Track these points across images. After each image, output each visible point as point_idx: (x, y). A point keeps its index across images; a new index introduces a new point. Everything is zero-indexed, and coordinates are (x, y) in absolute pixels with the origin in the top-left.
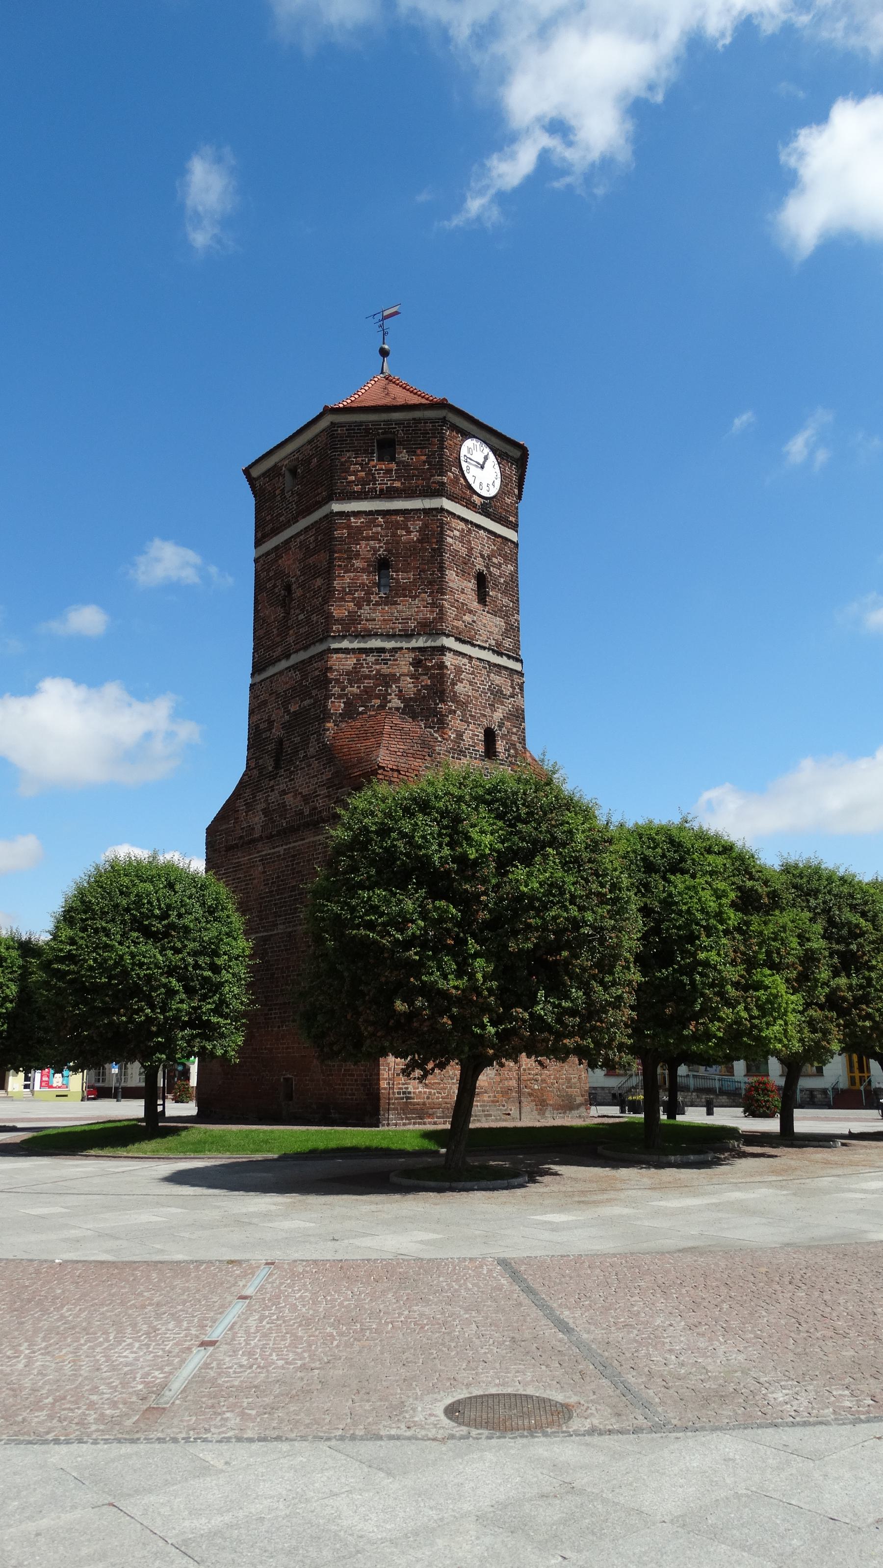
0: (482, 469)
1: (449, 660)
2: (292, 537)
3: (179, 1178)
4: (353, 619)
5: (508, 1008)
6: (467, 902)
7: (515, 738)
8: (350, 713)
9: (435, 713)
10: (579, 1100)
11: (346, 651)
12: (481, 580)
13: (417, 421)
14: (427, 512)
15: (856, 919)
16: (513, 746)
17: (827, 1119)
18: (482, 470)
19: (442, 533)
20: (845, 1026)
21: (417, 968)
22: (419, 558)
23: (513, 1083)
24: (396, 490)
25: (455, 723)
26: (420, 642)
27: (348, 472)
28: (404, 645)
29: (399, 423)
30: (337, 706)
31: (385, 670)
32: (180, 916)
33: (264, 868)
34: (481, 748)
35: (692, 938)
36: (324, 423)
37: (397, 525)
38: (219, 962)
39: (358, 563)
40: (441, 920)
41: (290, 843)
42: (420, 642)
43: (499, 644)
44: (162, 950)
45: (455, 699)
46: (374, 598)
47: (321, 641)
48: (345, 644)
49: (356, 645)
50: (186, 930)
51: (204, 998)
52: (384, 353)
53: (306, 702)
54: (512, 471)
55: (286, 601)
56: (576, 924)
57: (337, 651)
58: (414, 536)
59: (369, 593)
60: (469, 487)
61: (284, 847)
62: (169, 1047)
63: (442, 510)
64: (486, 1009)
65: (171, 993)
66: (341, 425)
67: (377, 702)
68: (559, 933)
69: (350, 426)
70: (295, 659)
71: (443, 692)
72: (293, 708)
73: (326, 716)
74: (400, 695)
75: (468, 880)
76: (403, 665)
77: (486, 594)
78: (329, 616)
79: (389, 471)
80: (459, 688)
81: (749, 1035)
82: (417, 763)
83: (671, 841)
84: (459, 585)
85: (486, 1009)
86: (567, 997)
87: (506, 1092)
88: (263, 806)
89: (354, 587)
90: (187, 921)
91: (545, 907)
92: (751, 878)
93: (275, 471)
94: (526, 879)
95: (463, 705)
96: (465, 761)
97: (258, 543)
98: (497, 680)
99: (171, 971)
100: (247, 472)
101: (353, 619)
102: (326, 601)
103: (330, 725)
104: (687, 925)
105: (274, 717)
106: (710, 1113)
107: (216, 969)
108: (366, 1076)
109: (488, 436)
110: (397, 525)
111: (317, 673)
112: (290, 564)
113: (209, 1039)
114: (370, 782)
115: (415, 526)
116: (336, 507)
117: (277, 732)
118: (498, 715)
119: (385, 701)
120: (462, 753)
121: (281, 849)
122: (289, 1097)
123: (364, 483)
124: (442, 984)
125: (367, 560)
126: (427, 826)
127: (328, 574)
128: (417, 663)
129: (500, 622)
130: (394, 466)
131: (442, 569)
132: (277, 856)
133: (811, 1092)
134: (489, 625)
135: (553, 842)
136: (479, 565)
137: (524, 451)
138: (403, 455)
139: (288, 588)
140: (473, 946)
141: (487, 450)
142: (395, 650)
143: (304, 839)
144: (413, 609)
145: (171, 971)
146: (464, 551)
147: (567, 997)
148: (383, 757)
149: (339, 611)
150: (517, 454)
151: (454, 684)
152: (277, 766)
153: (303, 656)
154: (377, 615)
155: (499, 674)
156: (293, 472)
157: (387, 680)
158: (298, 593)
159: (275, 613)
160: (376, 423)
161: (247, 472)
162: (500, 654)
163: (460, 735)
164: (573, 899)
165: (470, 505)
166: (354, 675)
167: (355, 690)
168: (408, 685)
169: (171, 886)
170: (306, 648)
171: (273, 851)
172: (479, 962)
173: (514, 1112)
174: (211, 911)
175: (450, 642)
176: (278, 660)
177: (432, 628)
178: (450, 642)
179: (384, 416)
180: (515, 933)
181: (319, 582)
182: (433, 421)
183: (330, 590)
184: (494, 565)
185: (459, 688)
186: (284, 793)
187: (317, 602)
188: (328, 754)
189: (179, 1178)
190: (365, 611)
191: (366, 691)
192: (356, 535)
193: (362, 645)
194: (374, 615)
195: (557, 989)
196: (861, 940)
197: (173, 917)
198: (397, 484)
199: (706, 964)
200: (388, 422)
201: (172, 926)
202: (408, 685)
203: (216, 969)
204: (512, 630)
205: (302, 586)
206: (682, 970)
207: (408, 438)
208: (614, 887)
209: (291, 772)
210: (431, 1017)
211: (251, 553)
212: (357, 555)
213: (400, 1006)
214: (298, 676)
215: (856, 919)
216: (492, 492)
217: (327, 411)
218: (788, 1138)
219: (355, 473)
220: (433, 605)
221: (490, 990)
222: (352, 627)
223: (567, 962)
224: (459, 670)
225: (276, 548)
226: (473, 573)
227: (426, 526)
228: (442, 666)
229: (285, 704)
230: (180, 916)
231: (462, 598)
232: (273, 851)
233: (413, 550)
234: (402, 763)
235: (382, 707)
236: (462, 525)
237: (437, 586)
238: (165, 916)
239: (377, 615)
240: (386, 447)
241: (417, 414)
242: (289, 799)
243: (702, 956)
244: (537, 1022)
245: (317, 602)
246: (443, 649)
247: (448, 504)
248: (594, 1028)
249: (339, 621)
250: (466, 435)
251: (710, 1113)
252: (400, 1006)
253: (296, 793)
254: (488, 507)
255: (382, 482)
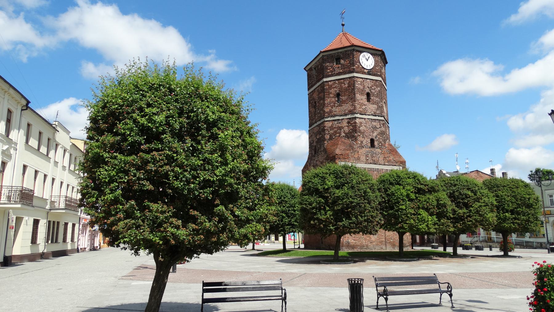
0: (367, 61)
1: (357, 121)
3: (278, 261)
4: (331, 111)
5: (337, 222)
6: (326, 198)
7: (381, 140)
8: (331, 138)
9: (354, 136)
10: (407, 244)
11: (329, 121)
12: (368, 95)
13: (346, 51)
14: (350, 78)
15: (469, 193)
16: (381, 142)
17: (542, 253)
18: (367, 61)
19: (354, 84)
20: (463, 224)
21: (315, 214)
22: (347, 92)
23: (384, 240)
24: (341, 73)
25: (360, 139)
26: (349, 116)
27: (327, 69)
28: (345, 117)
29: (341, 53)
30: (327, 137)
31: (340, 125)
32: (284, 198)
34: (369, 145)
35: (398, 202)
36: (321, 56)
37: (342, 83)
38: (295, 209)
39: (331, 95)
40: (320, 203)
42: (349, 116)
43: (375, 113)
44: (280, 207)
45: (360, 132)
46: (336, 105)
47: (323, 118)
48: (329, 119)
49: (332, 119)
50: (286, 202)
51: (292, 218)
52: (343, 25)
54: (379, 59)
55: (315, 107)
56: (352, 202)
57: (327, 121)
58: (346, 86)
59: (335, 104)
60: (363, 68)
62: (284, 230)
63: (354, 77)
64: (331, 223)
65: (283, 217)
66: (325, 56)
67: (338, 135)
68: (347, 205)
69: (327, 56)
71: (356, 130)
72: (318, 137)
73: (325, 140)
74: (344, 132)
75: (326, 193)
76: (345, 124)
77: (370, 98)
78: (324, 111)
79: (339, 67)
80: (361, 128)
81: (415, 228)
82: (348, 152)
83: (398, 176)
84: (361, 98)
85: (331, 223)
86: (351, 220)
87: (381, 242)
89: (330, 102)
90: (286, 199)
91: (343, 199)
92: (422, 184)
93: (311, 69)
94: (338, 193)
95: (363, 133)
96: (363, 149)
97: (309, 90)
98: (374, 124)
99: (283, 212)
100: (305, 69)
101: (331, 111)
102: (323, 107)
103: (326, 142)
104: (397, 199)
106: (491, 250)
107: (295, 211)
109: (369, 50)
110: (342, 83)
112: (315, 96)
113: (294, 228)
115: (347, 82)
116: (325, 80)
117: (315, 144)
118: (375, 134)
119: (340, 133)
120: (363, 147)
122: (322, 243)
123: (332, 72)
124: (321, 218)
125: (333, 94)
126: (316, 180)
127: (324, 99)
128: (348, 123)
129: (375, 106)
130: (340, 66)
131: (354, 94)
133: (541, 243)
134: (371, 107)
135: (348, 183)
136: (367, 90)
137: (382, 51)
138: (342, 61)
139: (315, 103)
140: (328, 208)
141: (369, 55)
142: (342, 119)
144: (347, 107)
145: (283, 212)
146: (362, 87)
147: (351, 220)
148: (338, 151)
149: (327, 110)
150: (380, 53)
151: (359, 127)
152: (315, 154)
154: (337, 110)
155: (375, 122)
156: (315, 69)
157: (340, 128)
158: (317, 105)
159: (313, 110)
160: (335, 53)
161: (305, 69)
162: (376, 116)
163: (362, 142)
164: (351, 197)
165: (363, 73)
166: (332, 128)
167: (332, 132)
168: (346, 129)
169: (282, 190)
170: (320, 120)
172: (329, 212)
173: (384, 247)
174: (293, 196)
175: (358, 115)
177: (352, 112)
178: (358, 115)
179: (337, 51)
180: (336, 205)
181: (322, 101)
182: (351, 50)
183: (324, 104)
184: (373, 89)
185: (361, 128)
186: (317, 161)
187: (321, 107)
188: (325, 150)
189: (278, 261)
190: (334, 109)
191: (335, 132)
192: (330, 87)
193: (334, 119)
194: (336, 110)
195: (349, 218)
196: (469, 199)
197: (282, 199)
198: (341, 71)
199: (402, 209)
200: (338, 53)
201: (282, 200)
202: (346, 129)
203: (295, 211)
204: (380, 108)
205: (318, 102)
206: (397, 211)
207: (345, 56)
208: (365, 192)
210: (319, 225)
211: (307, 92)
212: (331, 93)
213: (312, 222)
214: (318, 128)
215: (469, 193)
216: (371, 67)
217: (321, 52)
218: (455, 255)
219: (329, 69)
220: (352, 105)
221: (332, 219)
222: (331, 114)
223: (351, 211)
224: (361, 123)
226: (365, 93)
227: (349, 82)
228: (355, 123)
229: (316, 136)
230: (284, 198)
231: (361, 102)
233: (346, 90)
234: (343, 152)
235: (339, 136)
236: (361, 80)
237: (353, 99)
238: (280, 198)
239: (337, 110)
240: (338, 60)
241: (346, 49)
243: (400, 207)
244: (344, 226)
245: (321, 107)
246: (355, 118)
247: (355, 75)
248: (359, 227)
249: (327, 113)
250: (361, 52)
251: (491, 250)
252: (312, 222)
254: (370, 72)
255: (337, 70)
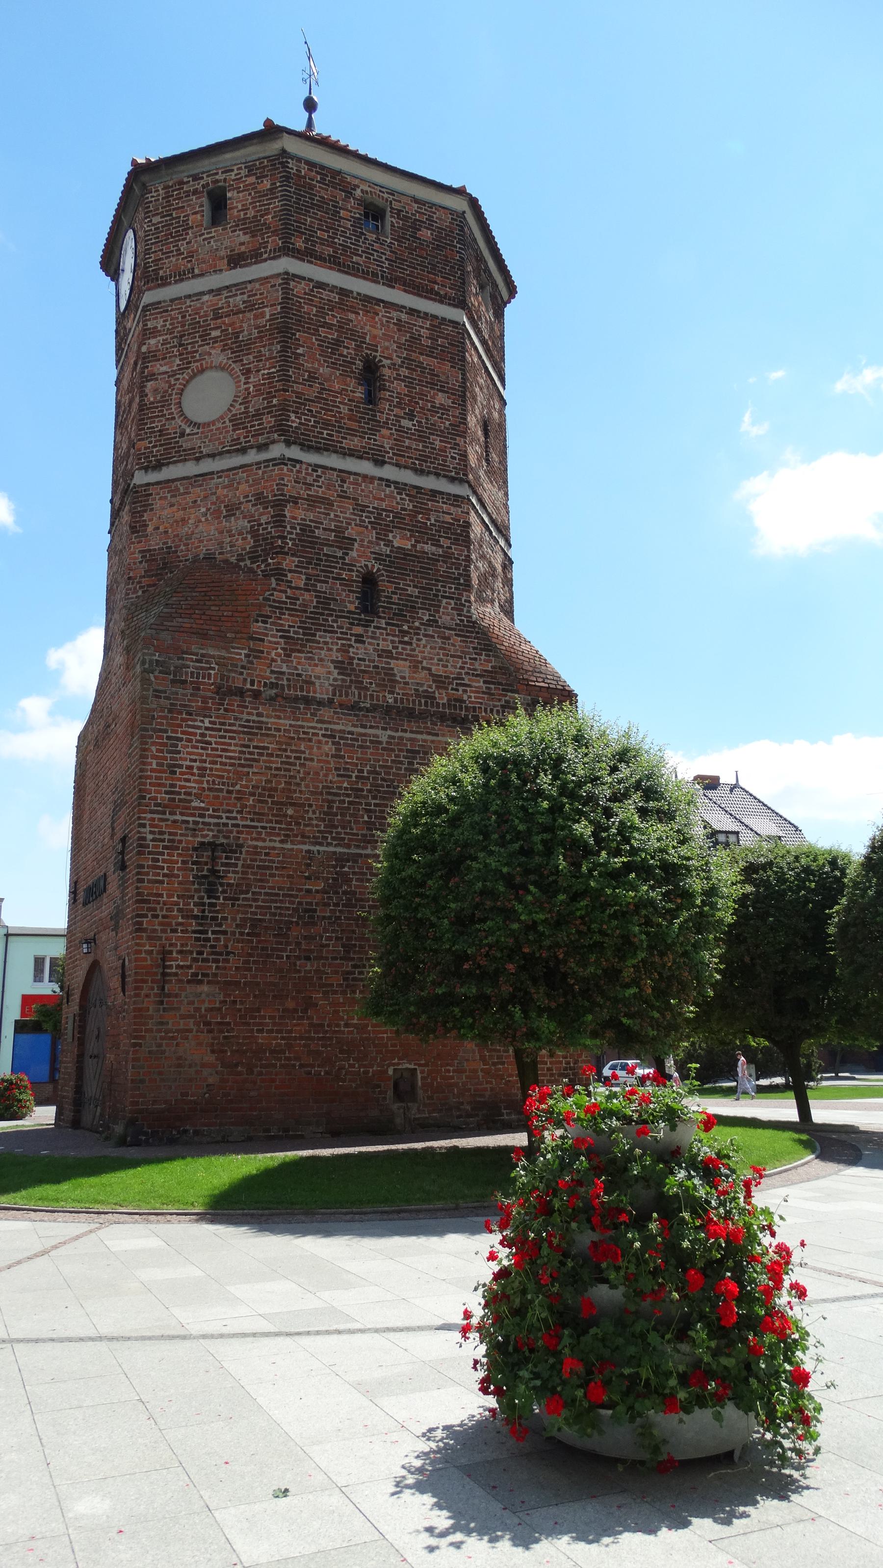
2: (383, 301)
33: (339, 750)
41: (405, 731)
53: (428, 548)
61: (389, 732)
70: (389, 472)
88: (336, 656)
105: (351, 532)
108: (568, 1063)
111: (448, 518)
114: (560, 702)
121: (384, 736)
132: (371, 742)
143: (437, 735)
153: (408, 477)
171: (363, 731)
176: (358, 454)
209: (404, 633)
225: (344, 293)
232: (363, 731)
242: (401, 668)
253: (415, 665)
